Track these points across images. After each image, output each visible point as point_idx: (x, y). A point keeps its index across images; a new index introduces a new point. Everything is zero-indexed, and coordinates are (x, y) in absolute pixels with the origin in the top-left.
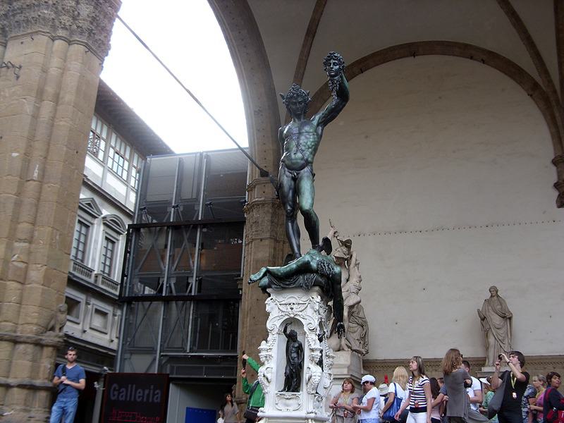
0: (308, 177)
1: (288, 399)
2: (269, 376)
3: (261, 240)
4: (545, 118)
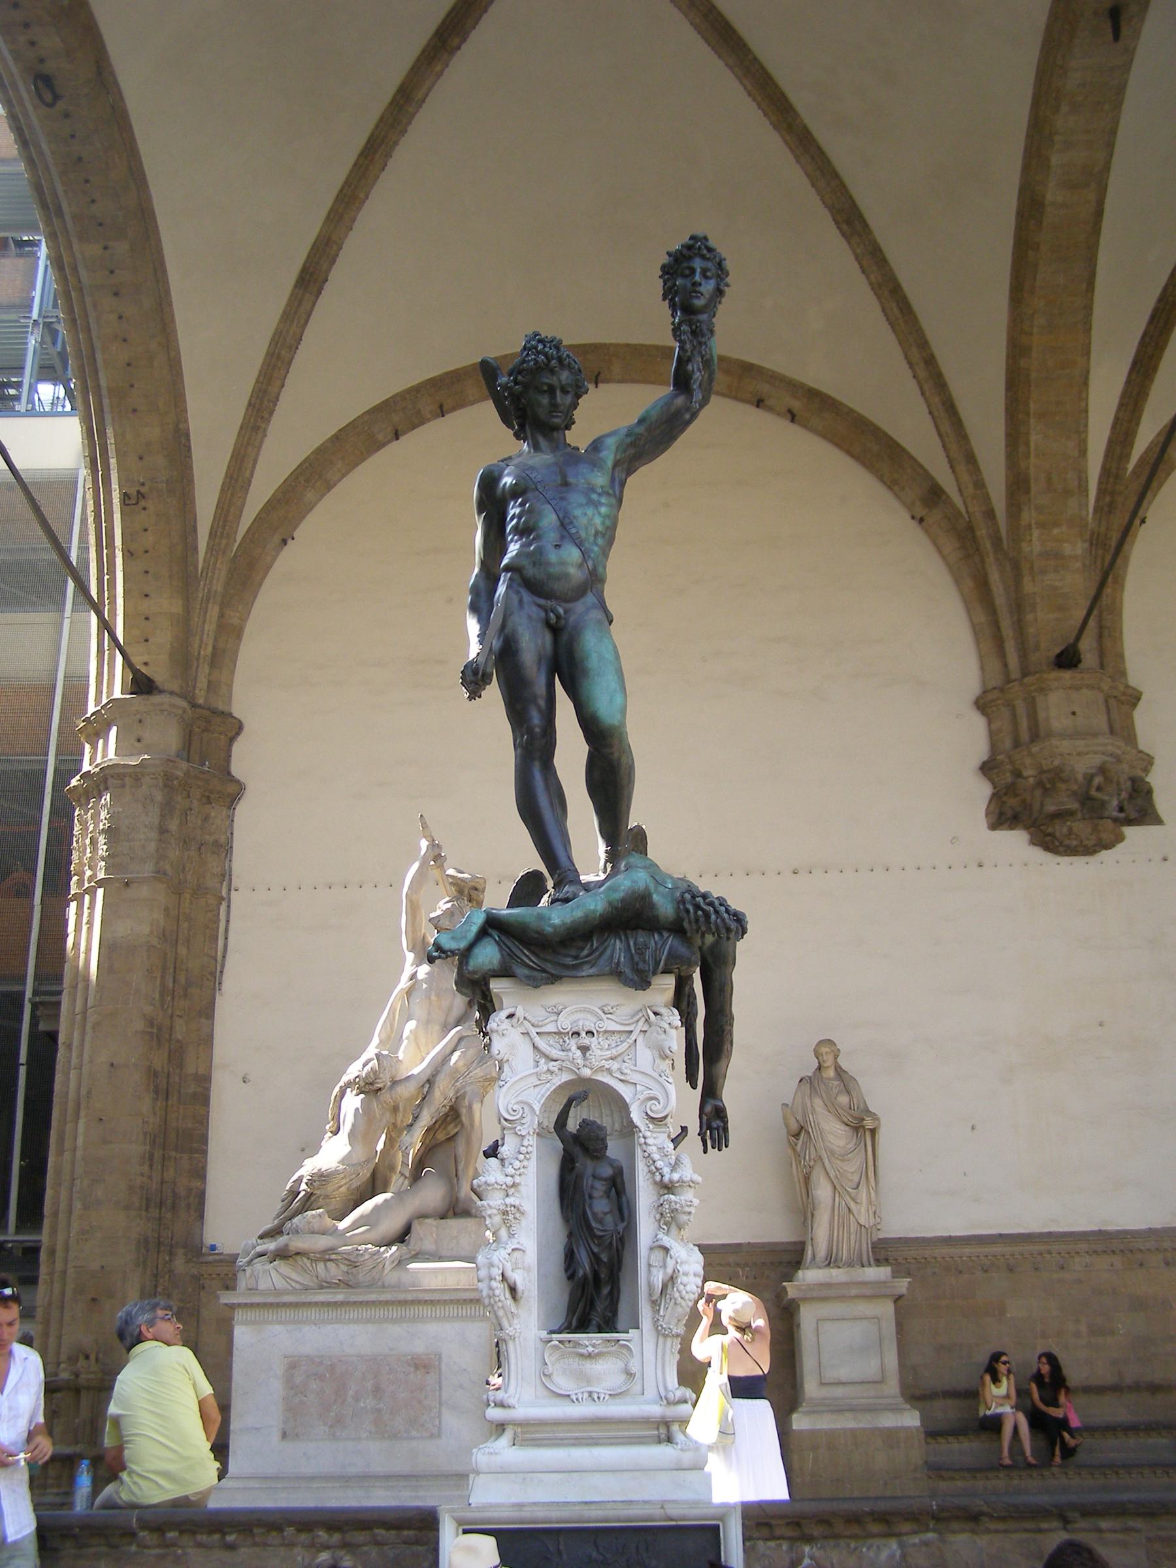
2: (517, 1277)
3: (127, 884)
4: (957, 581)
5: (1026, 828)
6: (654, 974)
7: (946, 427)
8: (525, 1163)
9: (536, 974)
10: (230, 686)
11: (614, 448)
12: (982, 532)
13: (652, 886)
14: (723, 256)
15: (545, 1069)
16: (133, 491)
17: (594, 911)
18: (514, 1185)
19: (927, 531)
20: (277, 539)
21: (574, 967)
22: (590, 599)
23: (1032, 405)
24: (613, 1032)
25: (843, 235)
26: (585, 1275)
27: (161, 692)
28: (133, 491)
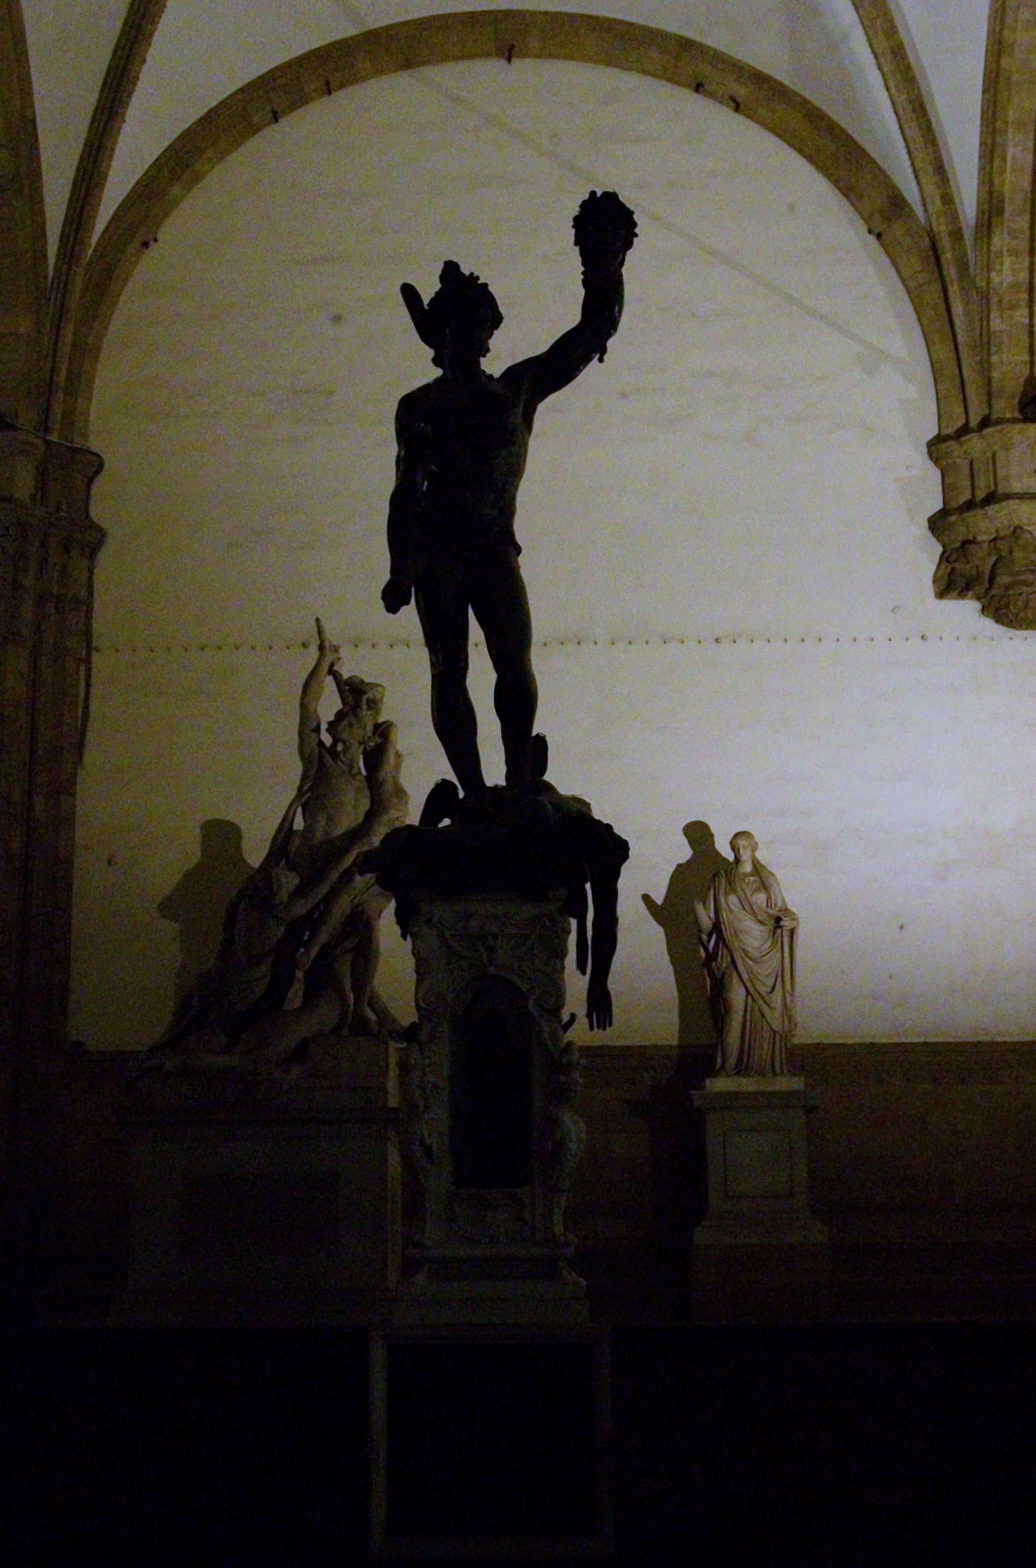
20: (137, 242)
23: (1011, 112)
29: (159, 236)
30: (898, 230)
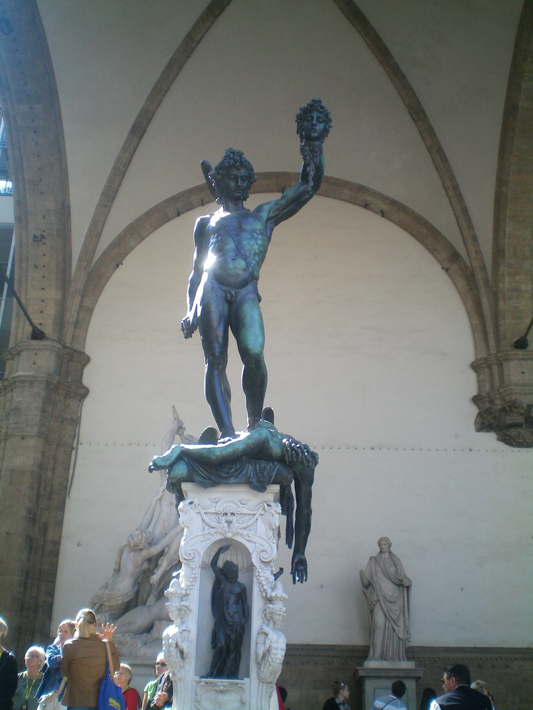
0: (253, 300)
1: (221, 692)
2: (184, 646)
3: (23, 438)
4: (465, 302)
5: (496, 432)
6: (268, 484)
7: (462, 221)
8: (193, 583)
9: (206, 481)
10: (85, 339)
11: (267, 211)
12: (479, 277)
13: (270, 437)
14: (329, 111)
15: (208, 532)
16: (38, 234)
17: (238, 449)
18: (187, 595)
19: (450, 276)
21: (226, 478)
22: (249, 287)
24: (246, 514)
25: (414, 120)
26: (221, 646)
27: (48, 339)
28: (38, 234)
29: (124, 262)
30: (455, 268)
